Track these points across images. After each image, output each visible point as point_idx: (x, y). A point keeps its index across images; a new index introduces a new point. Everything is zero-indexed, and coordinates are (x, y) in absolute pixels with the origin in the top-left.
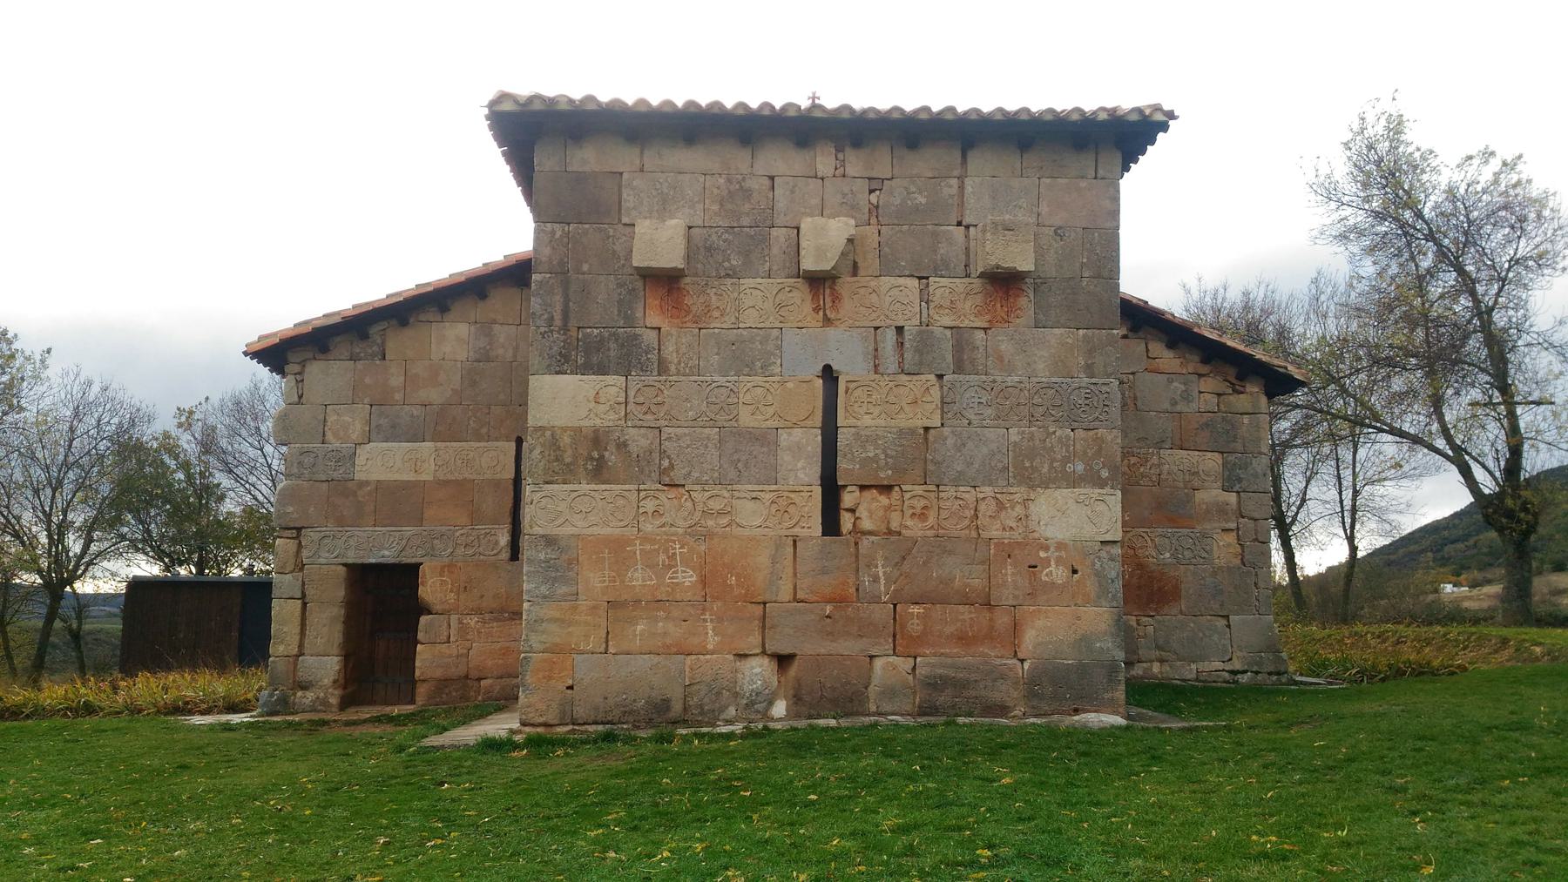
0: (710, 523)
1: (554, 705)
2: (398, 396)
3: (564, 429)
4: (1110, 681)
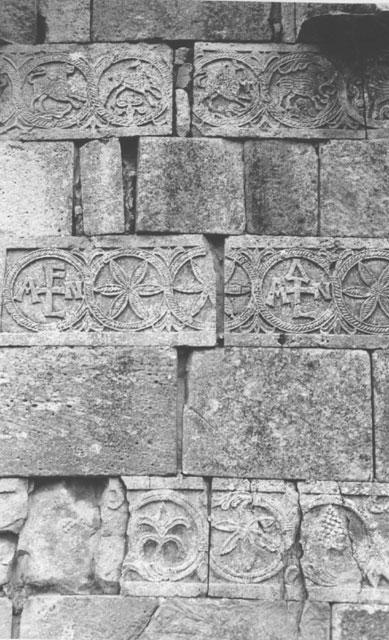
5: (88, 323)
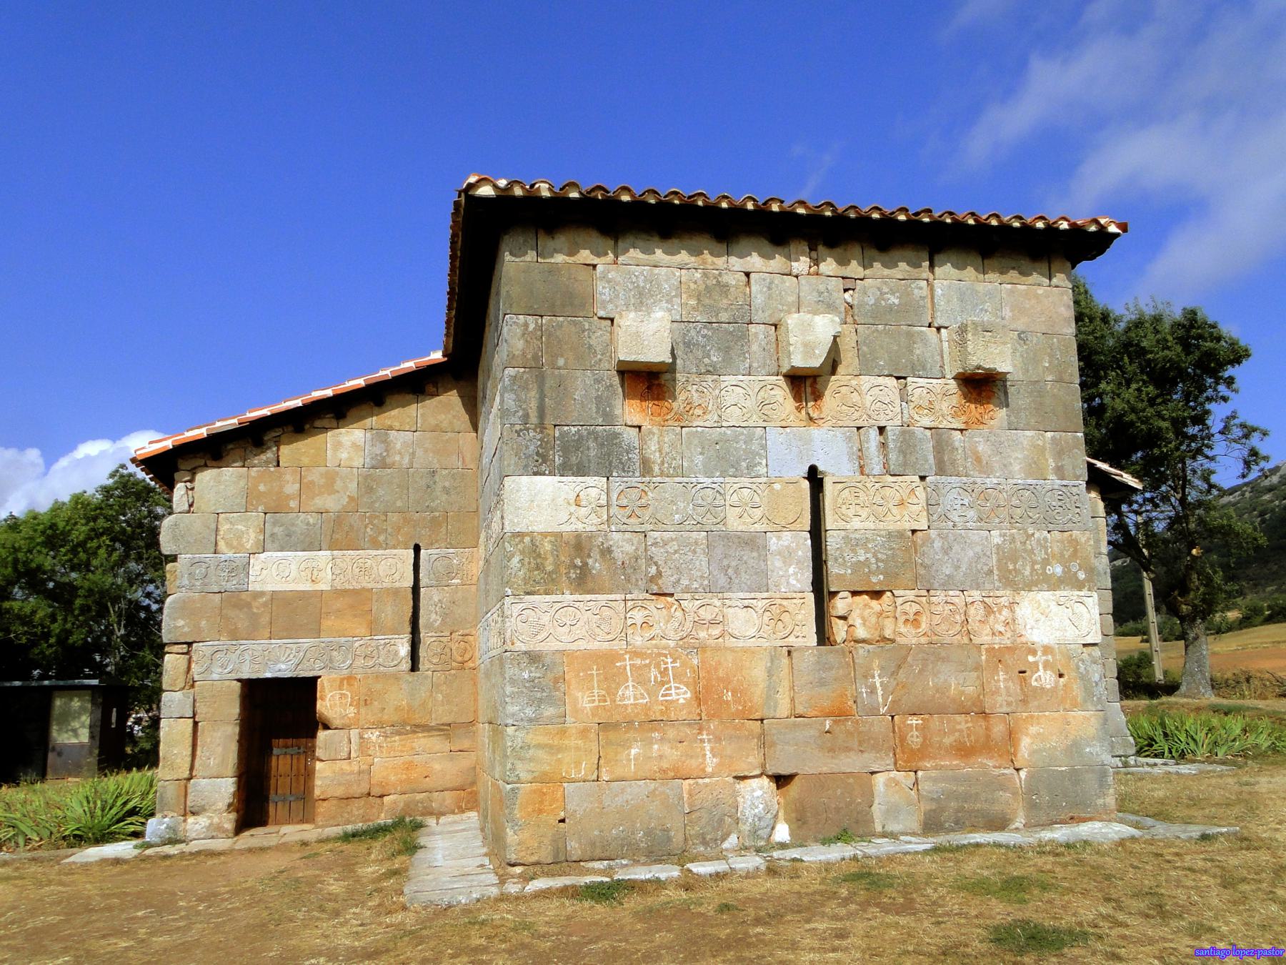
0: (702, 634)
1: (546, 841)
2: (293, 504)
3: (545, 535)
4: (1101, 786)
5: (872, 518)
